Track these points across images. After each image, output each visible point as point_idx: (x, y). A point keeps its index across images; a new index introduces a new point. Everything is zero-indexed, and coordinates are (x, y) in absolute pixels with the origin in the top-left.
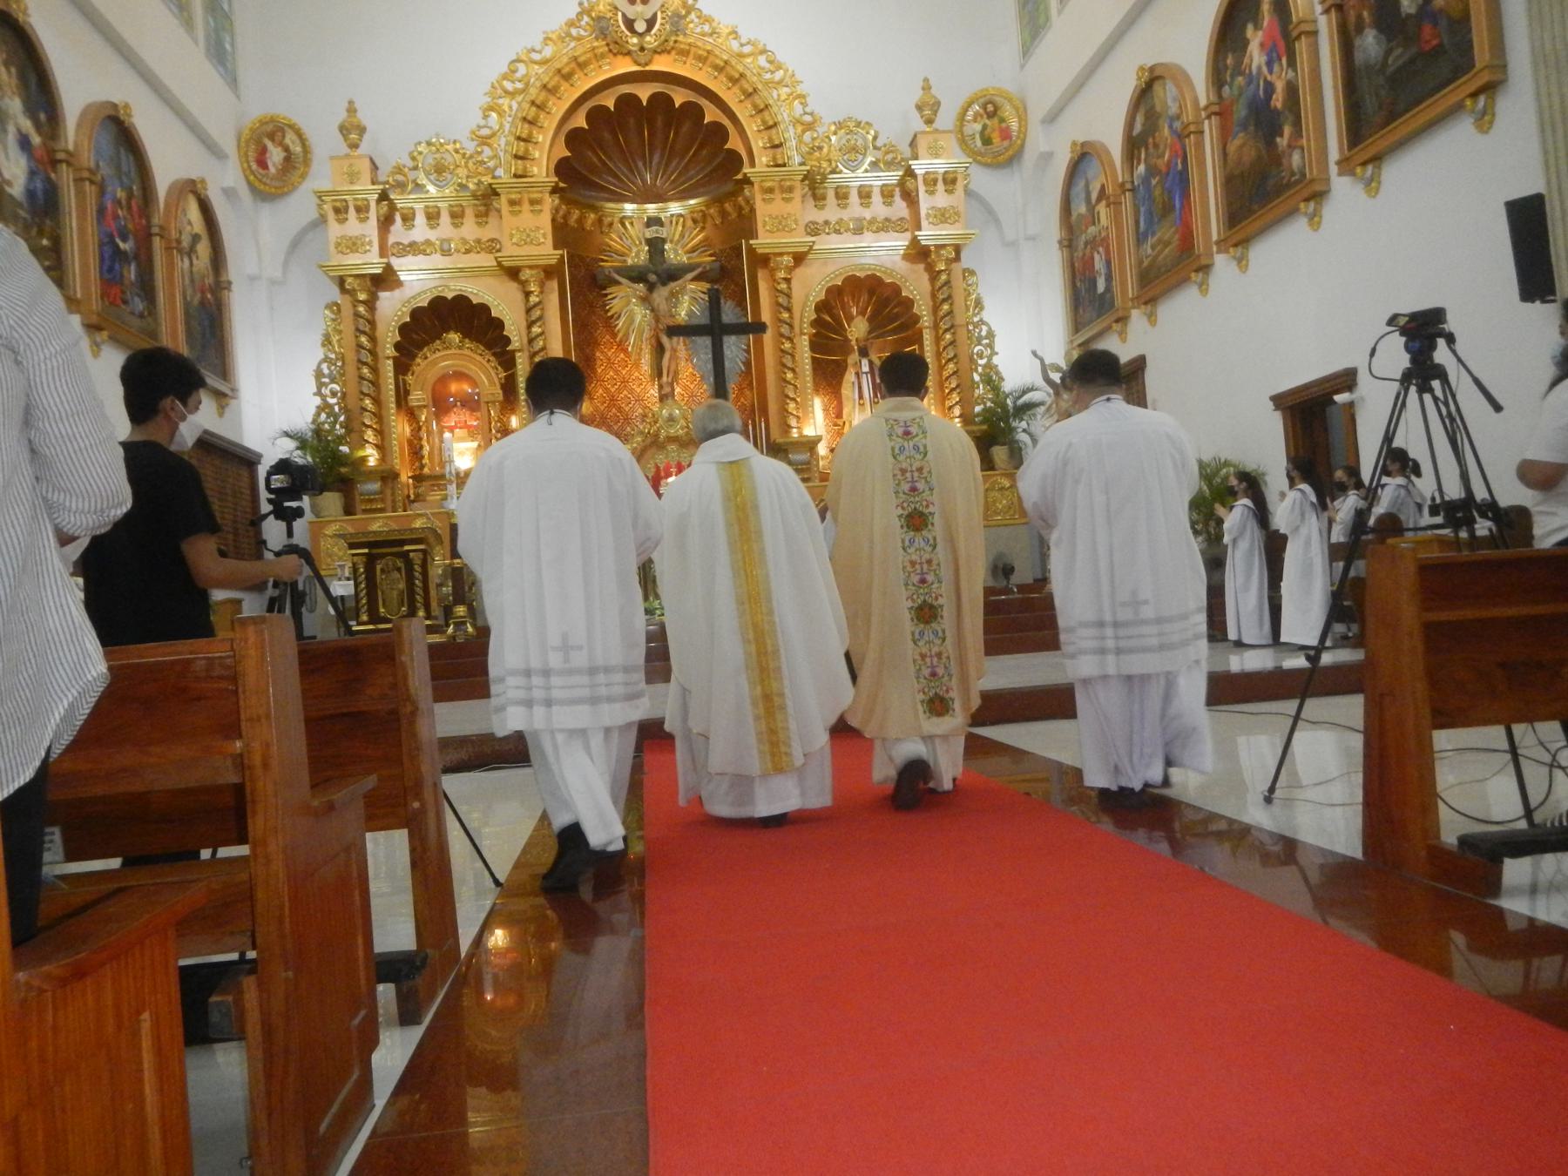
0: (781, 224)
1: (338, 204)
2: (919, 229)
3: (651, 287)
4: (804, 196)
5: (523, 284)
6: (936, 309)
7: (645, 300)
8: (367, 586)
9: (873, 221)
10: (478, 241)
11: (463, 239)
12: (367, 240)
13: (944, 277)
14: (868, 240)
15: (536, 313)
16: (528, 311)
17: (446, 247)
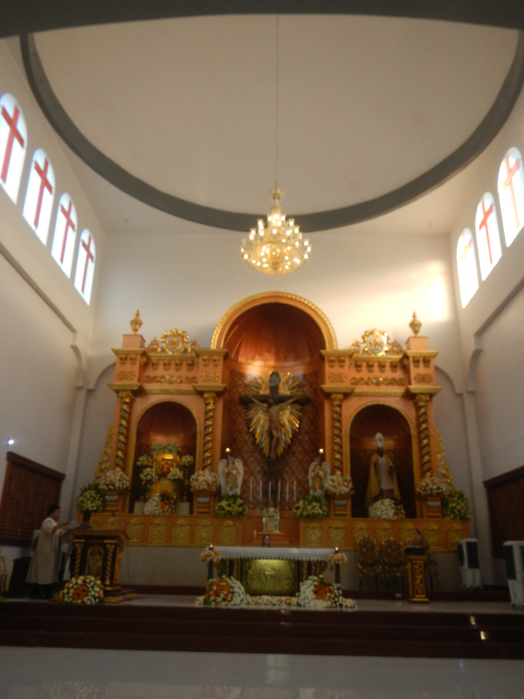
0: (339, 378)
1: (122, 356)
2: (410, 383)
3: (270, 406)
4: (351, 365)
5: (206, 399)
6: (419, 425)
7: (267, 411)
8: (80, 563)
9: (385, 379)
10: (187, 378)
11: (180, 377)
12: (133, 373)
13: (423, 410)
14: (384, 389)
15: (211, 414)
16: (206, 413)
17: (171, 379)
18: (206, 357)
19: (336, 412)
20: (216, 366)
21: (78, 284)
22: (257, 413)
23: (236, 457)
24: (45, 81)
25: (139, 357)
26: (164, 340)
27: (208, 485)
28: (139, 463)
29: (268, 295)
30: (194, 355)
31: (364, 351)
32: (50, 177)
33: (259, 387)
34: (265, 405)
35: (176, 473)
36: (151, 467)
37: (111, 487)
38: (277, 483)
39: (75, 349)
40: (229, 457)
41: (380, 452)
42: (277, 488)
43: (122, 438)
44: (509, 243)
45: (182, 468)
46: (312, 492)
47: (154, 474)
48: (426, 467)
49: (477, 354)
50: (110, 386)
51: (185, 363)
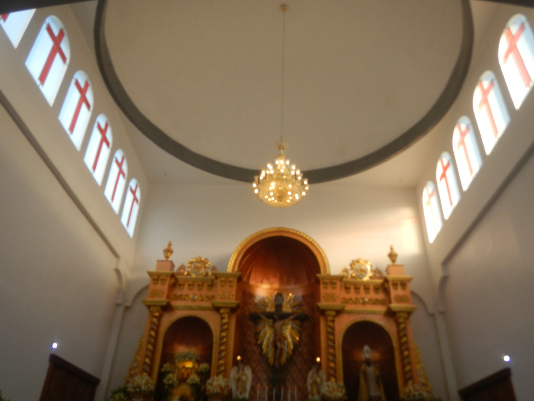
0: (332, 298)
3: (275, 321)
4: (341, 287)
5: (221, 314)
6: (400, 339)
7: (273, 326)
9: (370, 300)
10: (207, 297)
14: (369, 308)
15: (225, 327)
16: (222, 325)
18: (223, 279)
19: (330, 327)
20: (231, 286)
21: (124, 220)
22: (264, 327)
23: (245, 365)
24: (110, 65)
25: (168, 278)
26: (189, 265)
27: (221, 388)
28: (163, 370)
29: (274, 230)
30: (213, 277)
31: (352, 277)
32: (109, 135)
33: (265, 305)
34: (271, 321)
35: (195, 378)
36: (174, 373)
37: (138, 390)
38: (280, 390)
39: (117, 271)
40: (240, 364)
41: (368, 362)
42: (280, 395)
43: (150, 347)
44: (465, 188)
45: (200, 374)
46: (310, 397)
47: (175, 379)
48: (408, 376)
49: (445, 280)
50: (144, 302)
51: (206, 284)
